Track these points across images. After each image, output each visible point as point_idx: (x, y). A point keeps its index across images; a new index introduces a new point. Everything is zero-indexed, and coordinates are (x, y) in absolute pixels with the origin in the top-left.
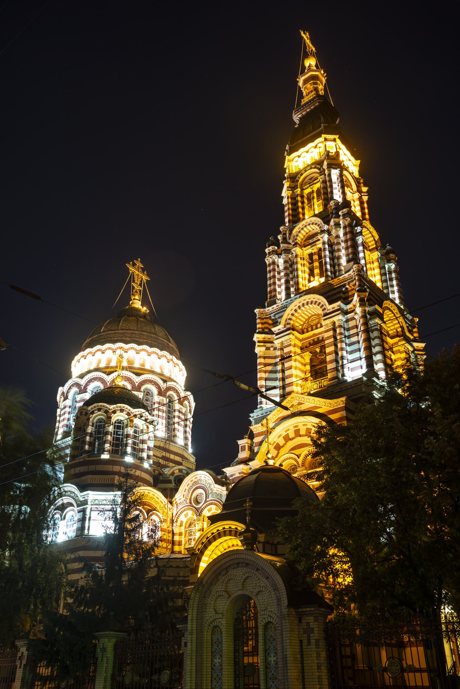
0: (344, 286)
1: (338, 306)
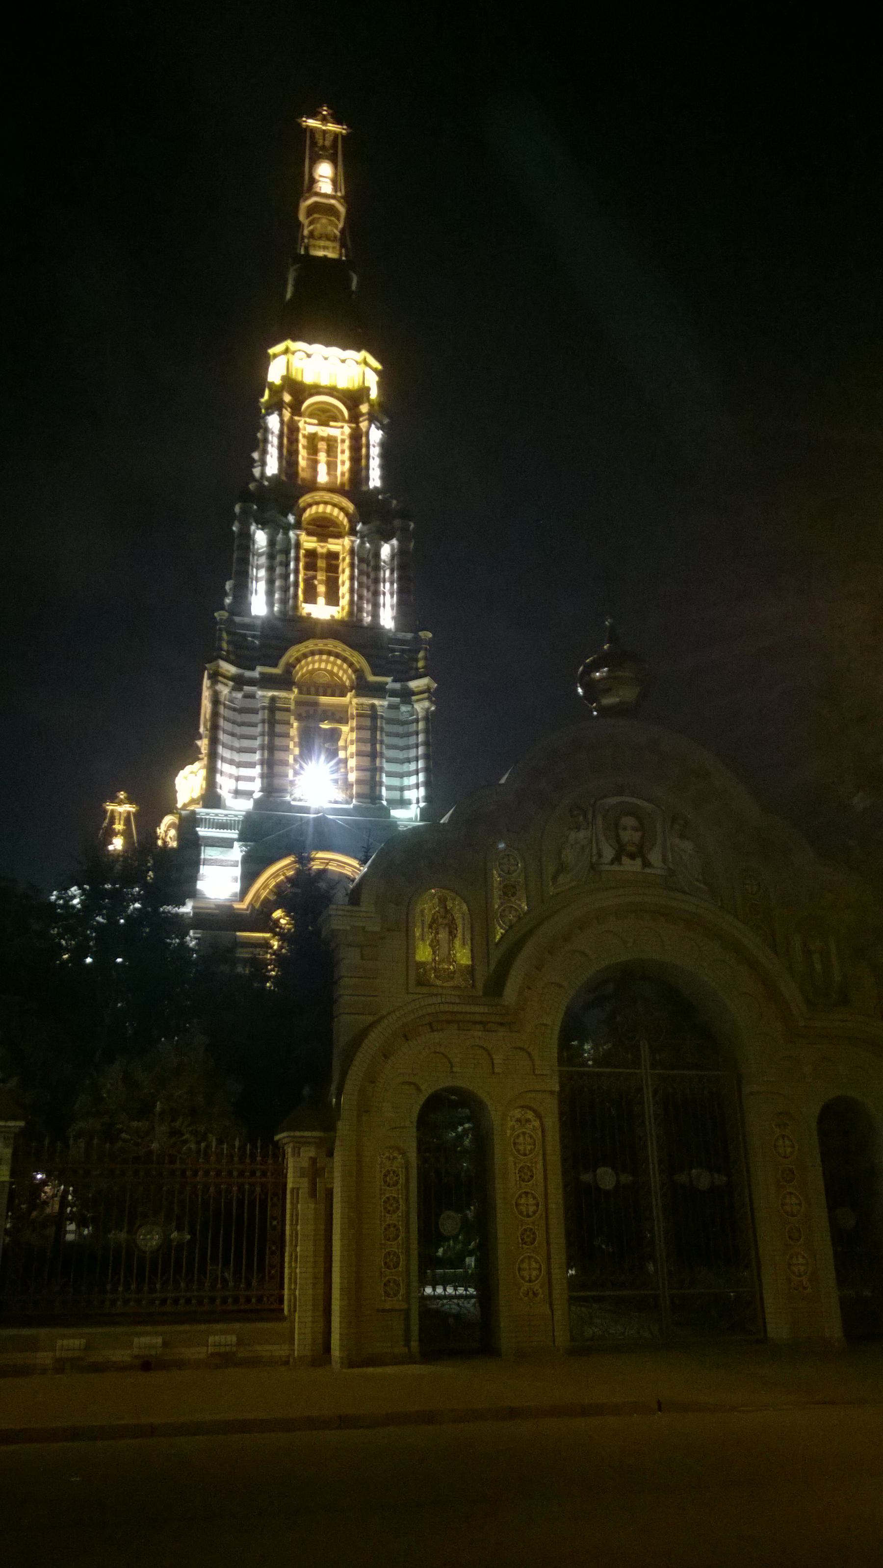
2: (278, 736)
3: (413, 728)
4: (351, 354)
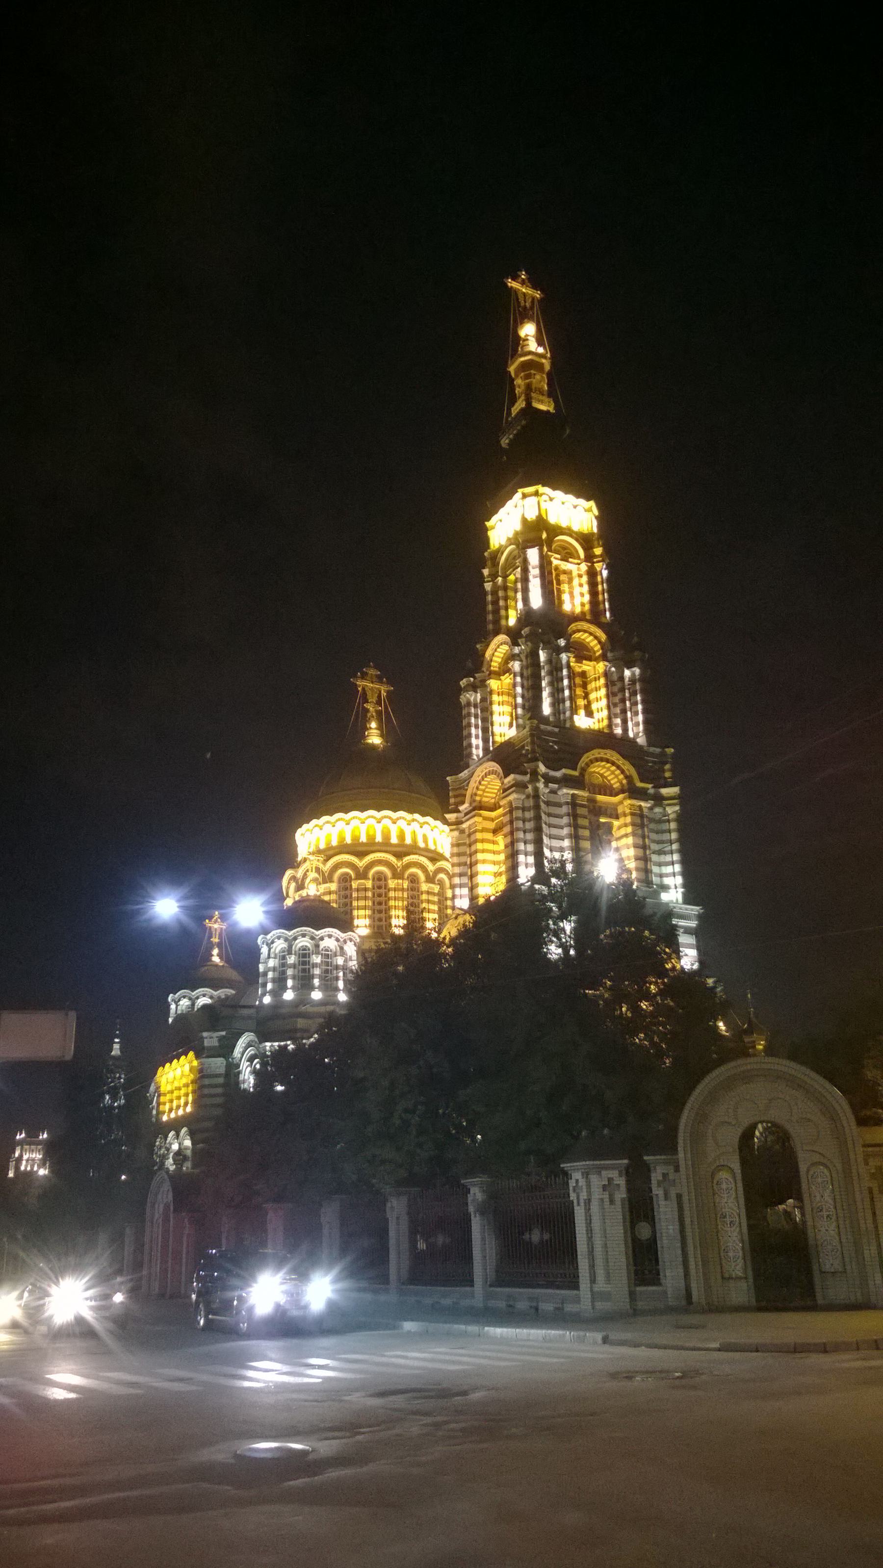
0: (523, 747)
1: (513, 780)
2: (582, 828)
3: (665, 826)
4: (581, 502)
